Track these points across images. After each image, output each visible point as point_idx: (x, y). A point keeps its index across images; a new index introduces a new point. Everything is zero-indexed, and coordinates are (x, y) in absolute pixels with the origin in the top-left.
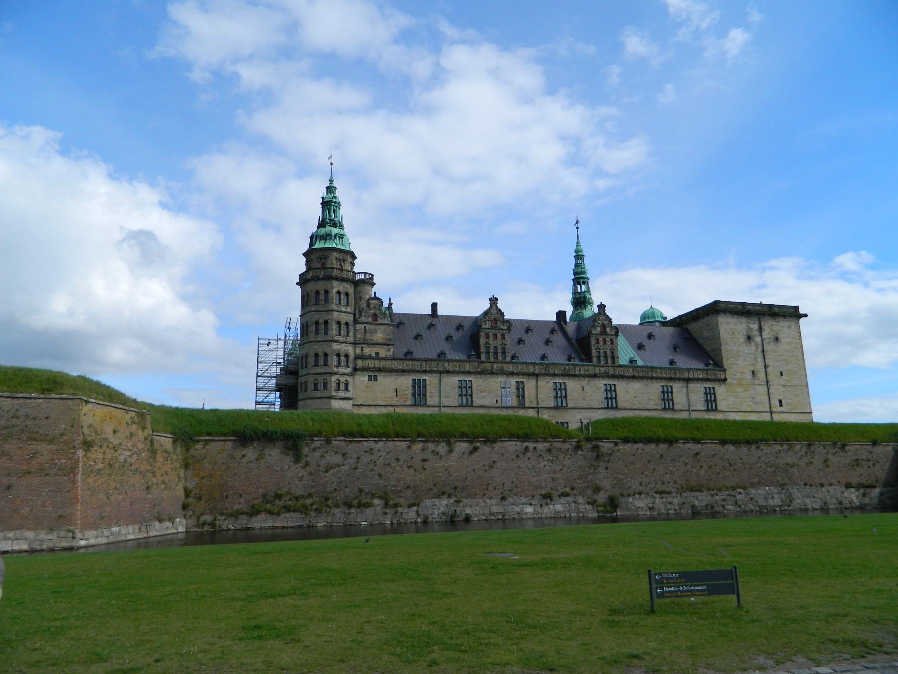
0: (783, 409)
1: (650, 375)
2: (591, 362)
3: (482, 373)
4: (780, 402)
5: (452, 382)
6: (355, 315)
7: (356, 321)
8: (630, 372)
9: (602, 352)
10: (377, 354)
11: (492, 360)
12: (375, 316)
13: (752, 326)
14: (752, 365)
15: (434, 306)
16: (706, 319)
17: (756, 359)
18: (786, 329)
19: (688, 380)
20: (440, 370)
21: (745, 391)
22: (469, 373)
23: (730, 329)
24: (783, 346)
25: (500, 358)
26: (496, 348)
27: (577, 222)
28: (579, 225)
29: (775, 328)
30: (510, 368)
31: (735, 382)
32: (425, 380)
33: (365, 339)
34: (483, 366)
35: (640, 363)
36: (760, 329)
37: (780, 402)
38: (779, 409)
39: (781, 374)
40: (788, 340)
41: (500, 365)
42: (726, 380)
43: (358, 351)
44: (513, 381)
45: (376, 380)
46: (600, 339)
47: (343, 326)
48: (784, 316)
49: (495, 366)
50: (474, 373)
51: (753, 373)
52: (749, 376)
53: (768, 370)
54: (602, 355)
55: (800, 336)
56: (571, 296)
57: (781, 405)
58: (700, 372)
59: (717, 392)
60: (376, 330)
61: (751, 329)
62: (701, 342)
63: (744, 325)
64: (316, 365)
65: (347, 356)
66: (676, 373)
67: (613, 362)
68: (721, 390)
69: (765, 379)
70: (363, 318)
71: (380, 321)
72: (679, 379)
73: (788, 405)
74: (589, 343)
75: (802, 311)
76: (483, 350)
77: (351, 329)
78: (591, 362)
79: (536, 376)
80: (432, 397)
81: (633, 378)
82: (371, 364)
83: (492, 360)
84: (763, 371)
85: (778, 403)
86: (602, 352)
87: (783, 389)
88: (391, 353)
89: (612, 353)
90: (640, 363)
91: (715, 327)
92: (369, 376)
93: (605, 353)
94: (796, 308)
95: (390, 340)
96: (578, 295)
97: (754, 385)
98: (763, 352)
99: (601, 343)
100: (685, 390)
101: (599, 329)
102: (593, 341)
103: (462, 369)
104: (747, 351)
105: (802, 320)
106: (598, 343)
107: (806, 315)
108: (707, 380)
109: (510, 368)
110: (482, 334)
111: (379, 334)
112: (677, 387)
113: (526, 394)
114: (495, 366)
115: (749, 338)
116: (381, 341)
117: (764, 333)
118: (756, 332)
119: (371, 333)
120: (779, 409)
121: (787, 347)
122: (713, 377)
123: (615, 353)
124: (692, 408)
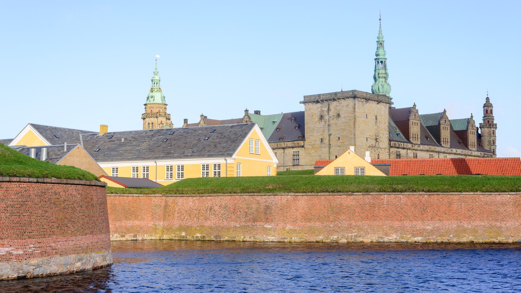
13: (324, 109)
14: (321, 135)
29: (337, 108)
36: (329, 110)
52: (318, 142)
61: (323, 111)
63: (319, 109)
87: (339, 148)
98: (329, 125)
104: (319, 126)
115: (321, 117)
117: (331, 113)
118: (326, 113)
121: (344, 120)
124: (285, 165)
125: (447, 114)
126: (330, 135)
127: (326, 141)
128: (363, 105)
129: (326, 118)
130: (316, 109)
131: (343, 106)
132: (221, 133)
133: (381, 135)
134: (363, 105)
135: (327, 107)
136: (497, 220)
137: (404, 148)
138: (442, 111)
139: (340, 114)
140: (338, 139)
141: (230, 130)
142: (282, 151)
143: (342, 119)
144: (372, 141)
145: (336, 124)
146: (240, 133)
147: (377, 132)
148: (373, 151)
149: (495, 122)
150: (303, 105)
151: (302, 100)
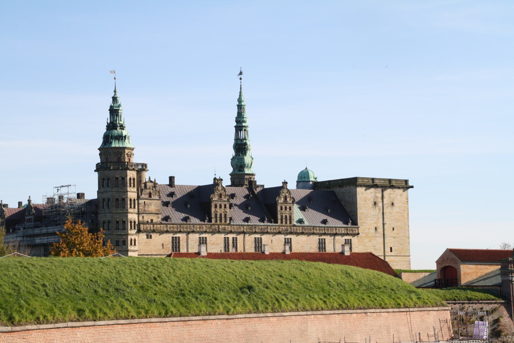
0: (392, 254)
1: (312, 232)
2: (276, 222)
3: (213, 233)
4: (391, 248)
5: (194, 238)
6: (138, 194)
7: (138, 197)
8: (300, 230)
9: (284, 215)
10: (152, 220)
11: (218, 222)
12: (150, 195)
14: (376, 223)
15: (172, 179)
16: (348, 188)
17: (378, 219)
18: (399, 196)
19: (336, 234)
20: (189, 230)
21: (370, 241)
22: (206, 232)
23: (364, 197)
24: (396, 209)
25: (223, 221)
26: (221, 215)
27: (241, 73)
28: (242, 76)
30: (229, 228)
31: (364, 235)
32: (179, 237)
33: (145, 210)
34: (213, 227)
35: (306, 223)
37: (391, 248)
38: (390, 254)
39: (393, 229)
41: (224, 226)
42: (358, 234)
43: (141, 219)
44: (231, 236)
45: (151, 238)
46: (284, 207)
47: (133, 202)
48: (399, 188)
49: (221, 227)
50: (209, 233)
51: (376, 228)
52: (373, 231)
53: (385, 226)
54: (284, 218)
55: (407, 202)
56: (233, 142)
57: (391, 251)
58: (343, 229)
59: (352, 242)
60: (151, 204)
61: (377, 197)
62: (343, 204)
63: (373, 195)
64: (117, 229)
65: (135, 222)
66: (328, 230)
67: (290, 223)
68: (355, 240)
69: (382, 233)
70: (143, 196)
71: (153, 197)
72: (331, 235)
73: (396, 251)
74: (276, 209)
75: (410, 184)
76: (213, 216)
77: (136, 202)
78: (277, 223)
79: (244, 233)
80: (183, 248)
81: (302, 233)
82: (149, 227)
83: (218, 222)
85: (389, 250)
86: (284, 215)
87: (393, 240)
88: (160, 219)
89: (290, 217)
90: (306, 223)
91: (354, 196)
92: (147, 236)
93: (286, 216)
94: (406, 181)
95: (159, 210)
96: (239, 142)
97: (376, 237)
99: (284, 209)
101: (283, 199)
102: (279, 208)
103: (201, 230)
104: (373, 214)
105: (410, 189)
106: (282, 209)
107: (412, 187)
108: (347, 234)
109: (229, 228)
110: (213, 205)
111: (153, 207)
112: (328, 239)
113: (238, 245)
114: (221, 227)
115: (375, 203)
116: (154, 211)
117: (385, 200)
119: (148, 206)
120: (390, 254)
121: (398, 210)
122: (351, 232)
123: (292, 216)
131: (396, 195)
139: (394, 203)
145: (390, 213)
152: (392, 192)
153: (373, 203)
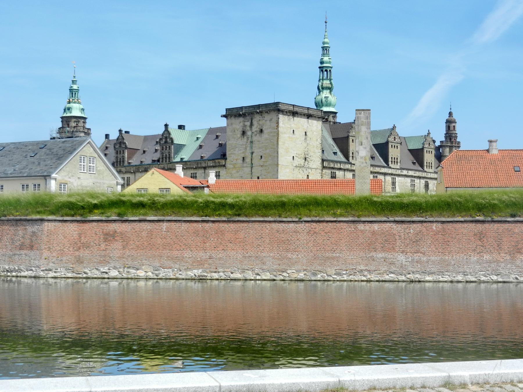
9: (164, 155)
14: (243, 153)
18: (268, 122)
29: (261, 123)
36: (252, 125)
39: (261, 157)
40: (269, 130)
46: (164, 147)
52: (240, 161)
59: (220, 174)
61: (245, 126)
63: (242, 124)
72: (199, 168)
84: (250, 156)
86: (164, 155)
87: (261, 168)
98: (252, 142)
100: (203, 175)
104: (241, 143)
115: (244, 133)
118: (248, 128)
121: (267, 136)
125: (397, 130)
126: (252, 153)
127: (248, 160)
128: (289, 120)
129: (249, 133)
130: (238, 124)
132: (50, 149)
133: (311, 154)
134: (289, 120)
135: (250, 121)
136: (288, 251)
137: (340, 169)
138: (391, 127)
139: (263, 129)
140: (260, 157)
141: (61, 145)
142: (202, 171)
143: (265, 135)
144: (299, 160)
145: (259, 141)
146: (69, 149)
147: (306, 150)
148: (301, 172)
149: (458, 140)
150: (225, 119)
151: (224, 113)
152: (261, 119)
153: (242, 133)
